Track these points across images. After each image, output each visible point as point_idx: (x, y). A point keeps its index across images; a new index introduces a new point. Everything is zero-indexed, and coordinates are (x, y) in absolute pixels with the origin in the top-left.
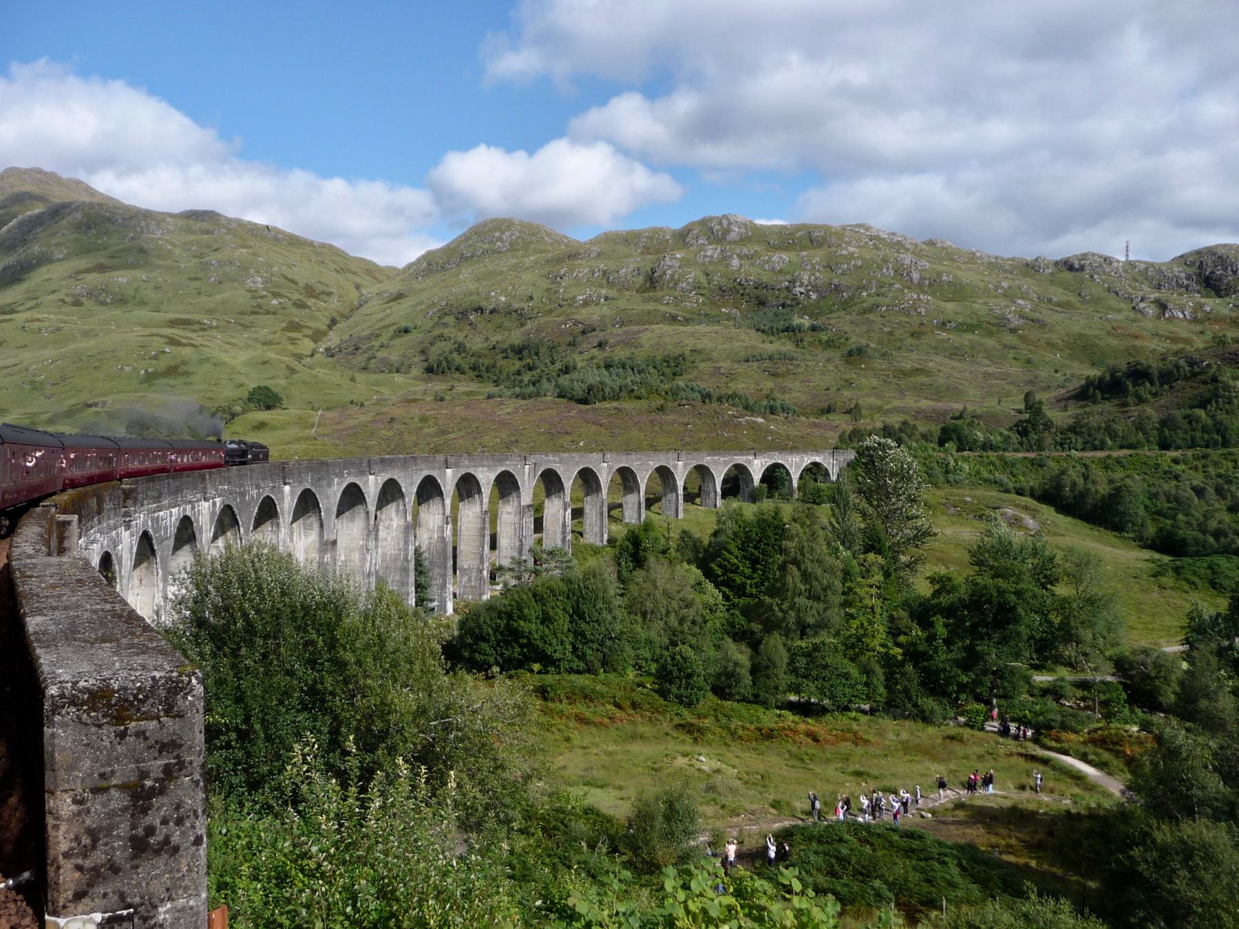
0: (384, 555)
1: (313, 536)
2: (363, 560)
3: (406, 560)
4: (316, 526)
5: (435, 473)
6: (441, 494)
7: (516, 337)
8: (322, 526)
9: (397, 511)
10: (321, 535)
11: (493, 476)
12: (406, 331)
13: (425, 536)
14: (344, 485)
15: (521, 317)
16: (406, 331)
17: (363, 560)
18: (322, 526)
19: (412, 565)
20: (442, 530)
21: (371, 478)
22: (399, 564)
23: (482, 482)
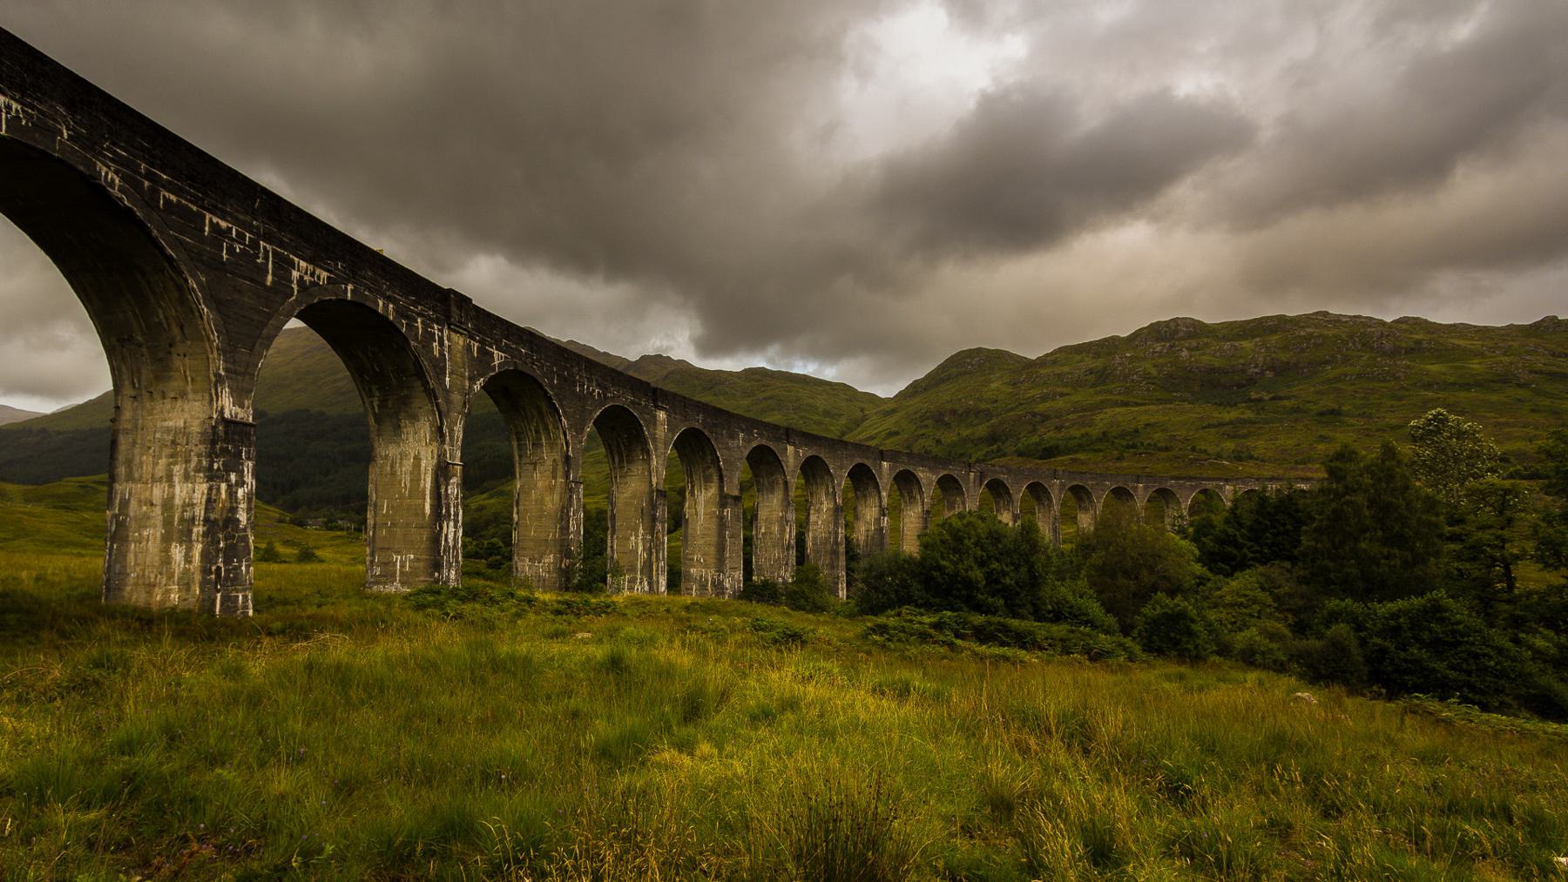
0: (815, 538)
1: (713, 490)
2: (782, 531)
3: (836, 542)
4: (715, 478)
5: (869, 463)
6: (877, 486)
7: (982, 430)
8: (721, 478)
9: (827, 494)
10: (721, 488)
11: (934, 478)
12: (897, 433)
13: (863, 529)
14: (754, 444)
15: (988, 415)
16: (897, 433)
17: (782, 531)
18: (721, 478)
19: (842, 549)
20: (878, 521)
21: (790, 449)
22: (829, 547)
23: (923, 481)
